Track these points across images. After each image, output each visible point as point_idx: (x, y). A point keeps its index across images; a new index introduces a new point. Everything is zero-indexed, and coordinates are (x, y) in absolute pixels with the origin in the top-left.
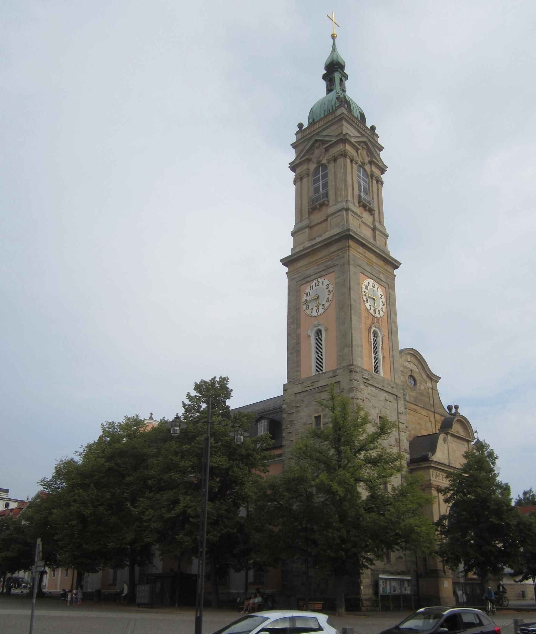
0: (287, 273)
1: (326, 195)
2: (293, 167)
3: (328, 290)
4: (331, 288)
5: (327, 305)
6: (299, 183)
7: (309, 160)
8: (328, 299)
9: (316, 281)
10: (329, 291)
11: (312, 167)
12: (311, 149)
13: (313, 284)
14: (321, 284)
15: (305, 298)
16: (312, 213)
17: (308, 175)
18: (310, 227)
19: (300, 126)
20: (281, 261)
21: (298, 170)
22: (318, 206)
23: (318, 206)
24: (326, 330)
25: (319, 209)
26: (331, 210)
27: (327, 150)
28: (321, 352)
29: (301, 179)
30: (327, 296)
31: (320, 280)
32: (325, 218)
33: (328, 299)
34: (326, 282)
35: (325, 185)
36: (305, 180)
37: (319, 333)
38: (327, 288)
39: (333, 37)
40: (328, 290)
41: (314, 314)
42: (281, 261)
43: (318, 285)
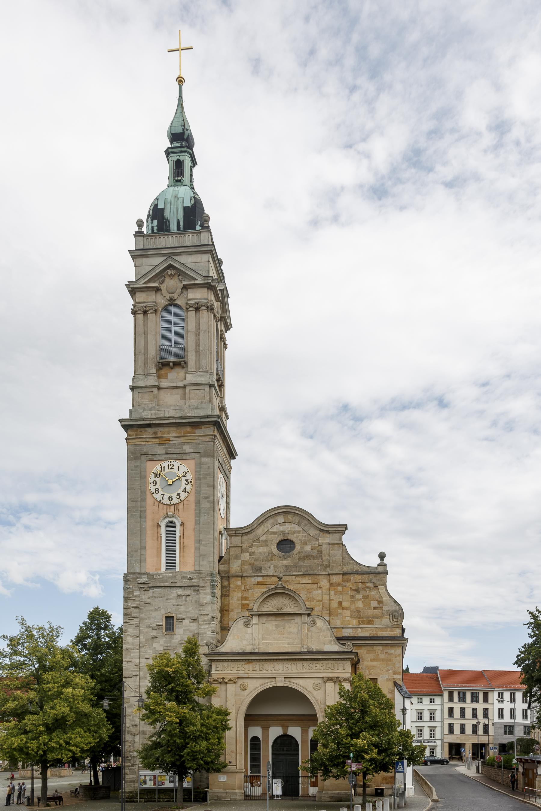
0: (126, 439)
1: (183, 352)
2: (133, 290)
3: (186, 478)
4: (189, 477)
5: (183, 495)
6: (140, 316)
7: (157, 290)
8: (185, 489)
9: (168, 462)
10: (187, 480)
11: (161, 301)
12: (161, 275)
13: (165, 464)
14: (176, 468)
15: (152, 478)
16: (161, 369)
17: (156, 311)
18: (159, 388)
19: (140, 223)
20: (120, 421)
21: (141, 297)
22: (171, 364)
23: (171, 364)
24: (182, 524)
25: (172, 368)
26: (190, 379)
27: (185, 287)
28: (174, 547)
29: (145, 313)
30: (184, 486)
31: (176, 463)
32: (181, 384)
33: (185, 489)
34: (183, 469)
35: (181, 335)
36: (151, 316)
37: (171, 525)
38: (184, 476)
39: (180, 81)
40: (186, 478)
41: (166, 501)
42: (120, 421)
43: (171, 469)
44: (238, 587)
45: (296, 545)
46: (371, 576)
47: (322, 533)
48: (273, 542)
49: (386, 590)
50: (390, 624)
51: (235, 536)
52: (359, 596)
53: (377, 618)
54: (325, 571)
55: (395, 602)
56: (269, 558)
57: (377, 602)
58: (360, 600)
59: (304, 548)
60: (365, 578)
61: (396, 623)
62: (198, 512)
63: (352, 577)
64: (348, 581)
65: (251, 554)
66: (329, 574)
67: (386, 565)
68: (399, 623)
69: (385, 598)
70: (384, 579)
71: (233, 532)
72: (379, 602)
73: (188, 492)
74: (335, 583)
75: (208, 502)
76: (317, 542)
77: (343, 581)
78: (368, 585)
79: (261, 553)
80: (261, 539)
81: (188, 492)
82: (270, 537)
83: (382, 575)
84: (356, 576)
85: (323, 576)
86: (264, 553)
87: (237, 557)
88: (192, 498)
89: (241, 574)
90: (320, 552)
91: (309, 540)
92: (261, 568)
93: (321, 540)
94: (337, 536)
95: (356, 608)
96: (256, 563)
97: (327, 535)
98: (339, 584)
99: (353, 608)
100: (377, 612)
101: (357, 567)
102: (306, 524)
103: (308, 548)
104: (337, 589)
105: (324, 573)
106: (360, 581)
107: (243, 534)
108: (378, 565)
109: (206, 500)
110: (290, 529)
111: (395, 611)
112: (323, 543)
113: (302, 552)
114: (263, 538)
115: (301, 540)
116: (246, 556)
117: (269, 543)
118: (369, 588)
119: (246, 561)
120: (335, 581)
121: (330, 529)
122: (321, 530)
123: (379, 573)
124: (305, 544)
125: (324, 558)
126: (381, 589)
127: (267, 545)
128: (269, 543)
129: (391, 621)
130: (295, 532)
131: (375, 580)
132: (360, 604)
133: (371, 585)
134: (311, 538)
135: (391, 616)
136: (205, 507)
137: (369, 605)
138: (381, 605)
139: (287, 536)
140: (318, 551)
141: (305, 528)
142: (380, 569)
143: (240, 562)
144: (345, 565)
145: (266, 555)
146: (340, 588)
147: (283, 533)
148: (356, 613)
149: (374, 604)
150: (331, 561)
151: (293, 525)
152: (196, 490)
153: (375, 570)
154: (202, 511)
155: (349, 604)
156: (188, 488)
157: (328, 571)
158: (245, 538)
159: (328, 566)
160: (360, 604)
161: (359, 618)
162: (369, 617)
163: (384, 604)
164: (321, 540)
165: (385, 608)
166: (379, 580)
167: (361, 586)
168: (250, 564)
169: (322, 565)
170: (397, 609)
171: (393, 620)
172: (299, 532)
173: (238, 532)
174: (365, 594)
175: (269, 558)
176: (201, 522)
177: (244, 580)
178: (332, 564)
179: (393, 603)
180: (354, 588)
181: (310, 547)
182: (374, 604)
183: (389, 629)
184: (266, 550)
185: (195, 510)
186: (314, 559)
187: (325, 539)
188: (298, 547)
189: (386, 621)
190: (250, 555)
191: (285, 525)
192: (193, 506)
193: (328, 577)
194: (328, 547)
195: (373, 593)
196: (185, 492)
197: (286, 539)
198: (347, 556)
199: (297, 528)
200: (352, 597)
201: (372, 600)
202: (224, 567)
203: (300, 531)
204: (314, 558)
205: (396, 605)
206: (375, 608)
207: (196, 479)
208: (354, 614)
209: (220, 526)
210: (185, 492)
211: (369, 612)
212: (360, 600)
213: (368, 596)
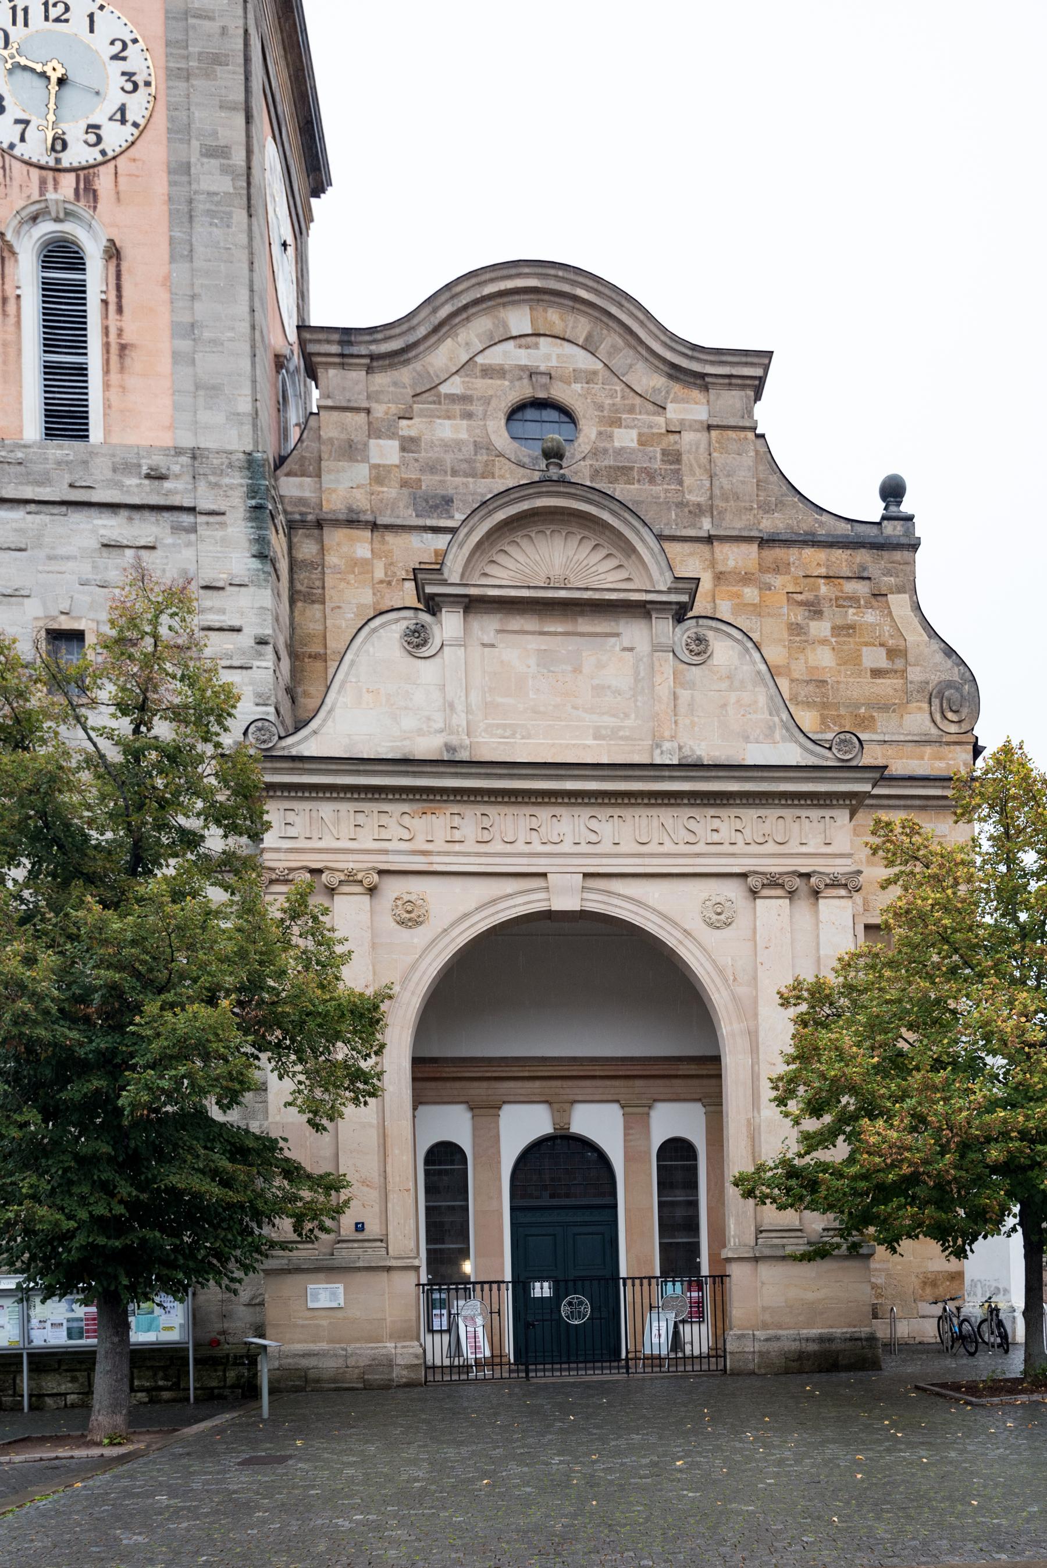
5: (115, 136)
8: (122, 109)
30: (115, 98)
33: (122, 109)
44: (355, 563)
45: (582, 423)
46: (863, 556)
47: (677, 388)
48: (494, 403)
49: (917, 608)
50: (934, 731)
51: (343, 365)
52: (820, 628)
53: (885, 708)
54: (693, 526)
55: (950, 652)
56: (479, 467)
57: (883, 651)
58: (824, 642)
59: (611, 437)
60: (841, 560)
61: (953, 728)
62: (184, 208)
63: (792, 554)
64: (777, 570)
65: (408, 445)
66: (709, 540)
67: (910, 518)
68: (965, 727)
69: (915, 636)
70: (908, 568)
71: (335, 349)
72: (892, 653)
73: (135, 125)
74: (734, 572)
75: (225, 170)
76: (661, 420)
77: (763, 569)
78: (850, 587)
79: (446, 446)
80: (444, 389)
81: (135, 125)
82: (482, 385)
83: (898, 555)
84: (808, 552)
85: (687, 547)
86: (459, 444)
87: (352, 451)
88: (155, 151)
89: (369, 517)
90: (673, 457)
91: (631, 410)
92: (448, 501)
93: (675, 412)
94: (733, 399)
95: (811, 669)
96: (429, 482)
97: (696, 394)
98: (746, 579)
99: (799, 670)
100: (887, 686)
101: (807, 522)
102: (614, 350)
103: (626, 438)
104: (738, 596)
105: (692, 533)
106: (823, 571)
107: (375, 362)
108: (884, 518)
109: (214, 162)
110: (561, 359)
111: (950, 685)
112: (682, 422)
113: (605, 451)
114: (454, 386)
115: (600, 407)
116: (386, 451)
117: (477, 408)
118: (854, 600)
119: (388, 468)
120: (731, 563)
121: (709, 369)
122: (676, 372)
123: (887, 541)
124: (617, 422)
125: (688, 481)
126: (899, 603)
127: (469, 415)
128: (477, 408)
129: (938, 717)
130: (578, 375)
131: (873, 571)
132: (824, 658)
133: (861, 589)
134: (638, 400)
135: (936, 702)
136: (213, 188)
137: (856, 659)
138: (899, 664)
139: (546, 387)
140: (665, 453)
141: (615, 363)
142: (892, 529)
143: (361, 472)
144: (766, 508)
145: (468, 451)
146: (750, 593)
147: (532, 374)
148: (811, 688)
149: (874, 657)
150: (717, 492)
151: (568, 349)
152: (171, 119)
153: (874, 531)
154: (200, 207)
155: (784, 652)
156: (137, 106)
157: (706, 525)
158: (381, 380)
159: (698, 511)
160: (824, 658)
161: (825, 706)
162: (858, 706)
163: (911, 658)
164: (675, 412)
165: (915, 674)
166: (888, 573)
167: (824, 589)
168: (404, 484)
169: (681, 505)
170: (957, 678)
171: (944, 717)
172: (590, 377)
173: (355, 350)
174: (839, 622)
175: (479, 467)
176: (200, 250)
177: (383, 542)
178: (719, 503)
179: (939, 657)
180: (799, 597)
181: (634, 434)
182: (874, 657)
183: (928, 750)
184: (464, 435)
185: (170, 199)
186: (652, 480)
187: (690, 408)
188: (589, 432)
189: (918, 720)
190: (403, 449)
191: (536, 346)
192: (160, 185)
193: (703, 548)
194: (702, 437)
195: (870, 617)
196: (123, 121)
197: (541, 395)
198: (775, 478)
199: (583, 360)
200: (796, 629)
201: (866, 644)
202: (301, 486)
203: (595, 373)
204: (651, 477)
205: (950, 663)
206: (877, 673)
207: (173, 74)
208: (803, 692)
209: (284, 338)
210: (123, 121)
211: (859, 688)
212: (824, 642)
213: (852, 627)
